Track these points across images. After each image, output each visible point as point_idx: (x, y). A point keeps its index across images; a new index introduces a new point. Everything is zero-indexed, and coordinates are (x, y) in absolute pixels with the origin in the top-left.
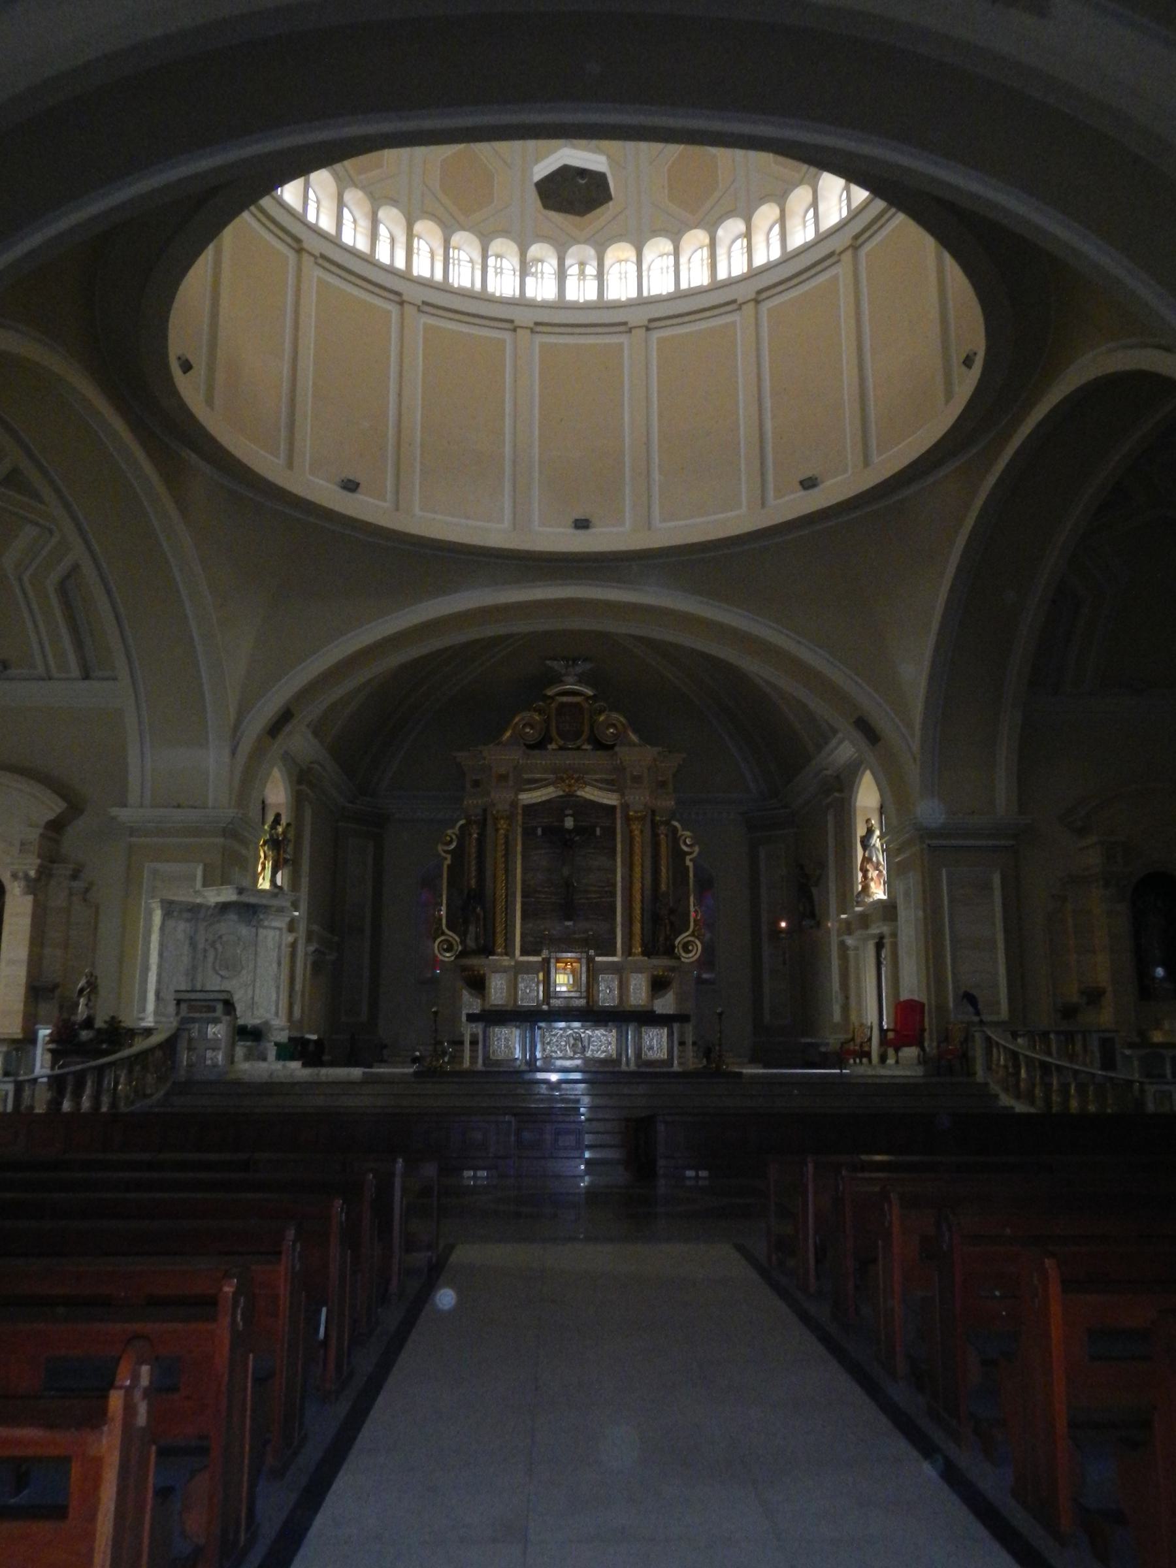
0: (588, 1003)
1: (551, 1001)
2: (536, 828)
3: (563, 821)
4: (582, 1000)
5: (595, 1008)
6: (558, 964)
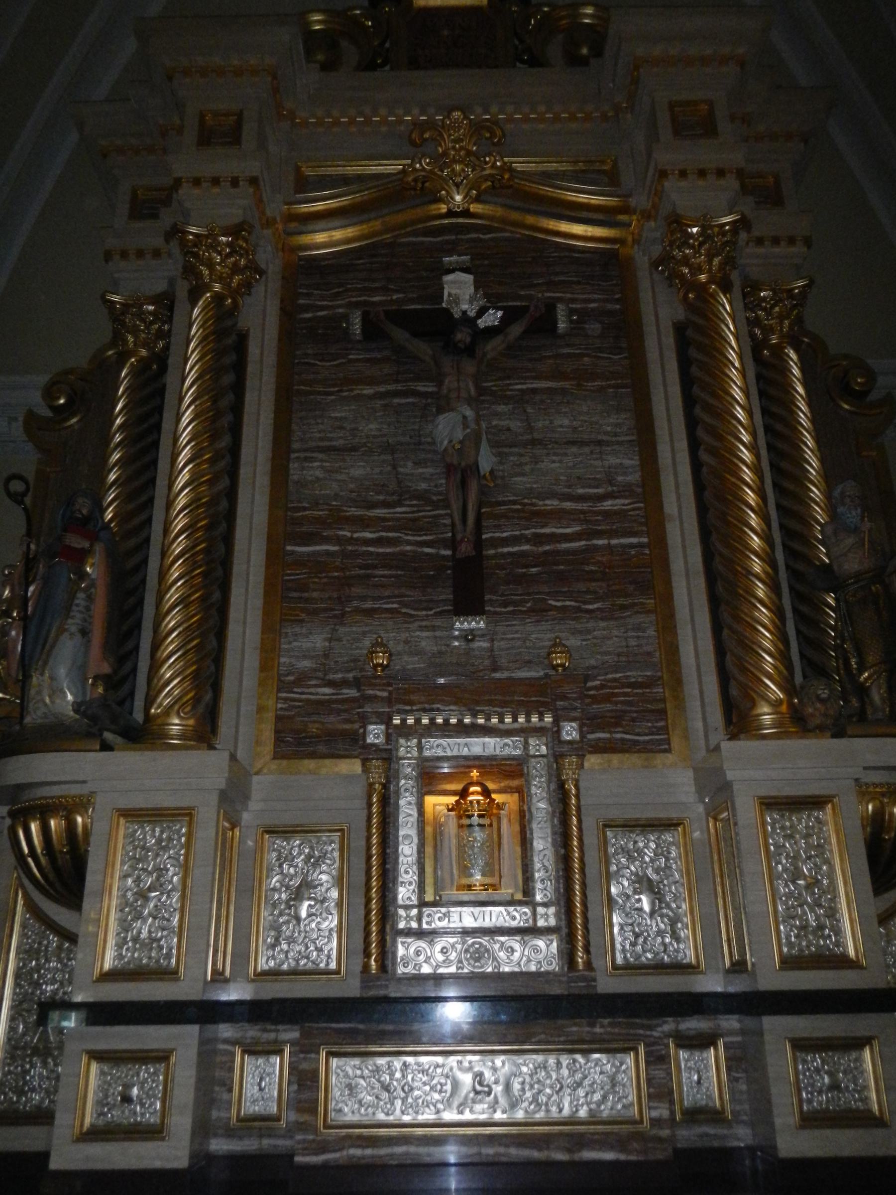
0: (568, 955)
1: (401, 951)
2: (345, 317)
3: (438, 296)
4: (541, 943)
5: (606, 985)
6: (430, 801)
